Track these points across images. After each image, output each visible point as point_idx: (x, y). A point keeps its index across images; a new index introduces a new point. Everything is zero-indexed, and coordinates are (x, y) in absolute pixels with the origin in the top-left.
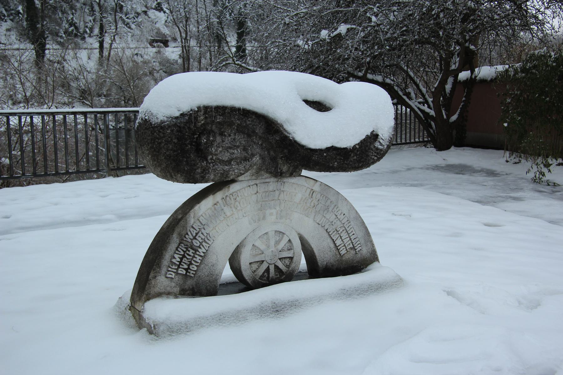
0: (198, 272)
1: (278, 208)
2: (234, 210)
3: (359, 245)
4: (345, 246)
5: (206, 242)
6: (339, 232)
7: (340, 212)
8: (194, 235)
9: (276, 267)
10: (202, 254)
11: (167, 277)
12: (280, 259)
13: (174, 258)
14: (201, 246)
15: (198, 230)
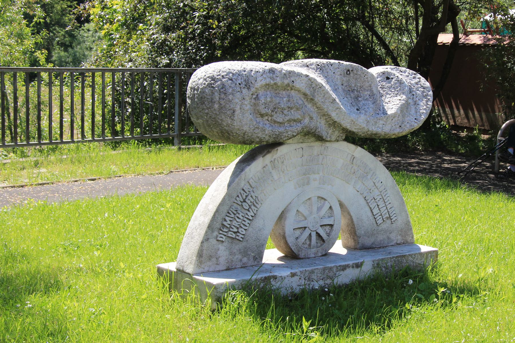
0: (246, 237)
1: (321, 174)
2: (281, 173)
3: (395, 215)
4: (381, 215)
5: (255, 206)
6: (377, 201)
7: (377, 180)
8: (244, 197)
9: (318, 235)
10: (251, 218)
11: (218, 240)
12: (321, 226)
13: (225, 220)
14: (250, 210)
15: (248, 192)
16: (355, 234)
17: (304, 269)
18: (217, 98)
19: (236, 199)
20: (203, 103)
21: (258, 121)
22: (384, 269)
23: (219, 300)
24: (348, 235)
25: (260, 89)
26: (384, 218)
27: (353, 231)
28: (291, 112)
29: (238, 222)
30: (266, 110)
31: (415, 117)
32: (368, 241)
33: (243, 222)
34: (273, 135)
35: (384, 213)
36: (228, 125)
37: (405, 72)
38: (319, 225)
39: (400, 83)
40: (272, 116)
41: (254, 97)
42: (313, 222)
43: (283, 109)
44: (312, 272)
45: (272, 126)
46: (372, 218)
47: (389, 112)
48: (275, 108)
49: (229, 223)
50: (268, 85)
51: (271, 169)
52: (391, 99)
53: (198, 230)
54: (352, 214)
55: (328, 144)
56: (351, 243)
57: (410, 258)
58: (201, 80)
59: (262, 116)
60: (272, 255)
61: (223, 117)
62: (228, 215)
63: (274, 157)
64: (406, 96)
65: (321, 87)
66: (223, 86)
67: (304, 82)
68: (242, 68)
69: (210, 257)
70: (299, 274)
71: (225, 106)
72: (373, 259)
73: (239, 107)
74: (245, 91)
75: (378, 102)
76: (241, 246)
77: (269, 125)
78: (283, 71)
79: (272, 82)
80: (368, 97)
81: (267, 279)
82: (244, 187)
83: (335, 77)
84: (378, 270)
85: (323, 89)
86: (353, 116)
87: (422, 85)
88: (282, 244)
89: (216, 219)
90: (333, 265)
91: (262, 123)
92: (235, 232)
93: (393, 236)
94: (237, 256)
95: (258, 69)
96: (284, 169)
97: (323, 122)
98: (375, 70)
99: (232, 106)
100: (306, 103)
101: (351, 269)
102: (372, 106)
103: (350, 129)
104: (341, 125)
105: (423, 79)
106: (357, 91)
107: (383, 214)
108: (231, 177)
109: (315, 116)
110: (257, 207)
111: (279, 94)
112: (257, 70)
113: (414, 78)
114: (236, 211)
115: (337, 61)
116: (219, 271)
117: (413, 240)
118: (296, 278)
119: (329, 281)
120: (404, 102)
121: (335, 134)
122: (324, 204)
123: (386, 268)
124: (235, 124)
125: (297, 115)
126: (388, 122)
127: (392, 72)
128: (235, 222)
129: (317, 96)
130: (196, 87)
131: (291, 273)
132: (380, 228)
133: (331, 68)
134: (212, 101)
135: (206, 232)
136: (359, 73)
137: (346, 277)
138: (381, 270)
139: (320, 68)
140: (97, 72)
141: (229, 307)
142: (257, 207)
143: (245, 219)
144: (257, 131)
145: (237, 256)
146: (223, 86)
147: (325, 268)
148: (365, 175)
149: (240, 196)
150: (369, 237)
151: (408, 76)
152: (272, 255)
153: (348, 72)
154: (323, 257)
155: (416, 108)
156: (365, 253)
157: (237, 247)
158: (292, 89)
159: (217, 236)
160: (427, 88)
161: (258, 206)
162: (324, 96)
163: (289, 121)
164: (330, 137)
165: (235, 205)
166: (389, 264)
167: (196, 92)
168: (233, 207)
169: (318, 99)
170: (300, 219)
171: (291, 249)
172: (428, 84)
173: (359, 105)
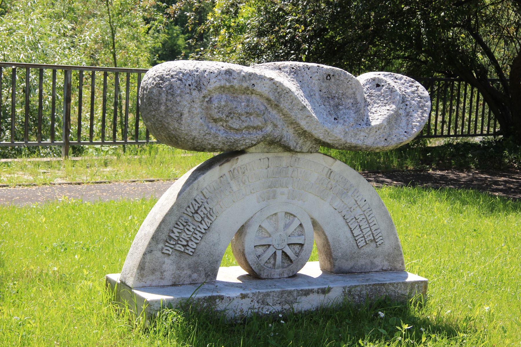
0: (197, 251)
1: (290, 187)
2: (241, 185)
3: (381, 238)
4: (364, 237)
5: (208, 218)
6: (359, 221)
7: (360, 198)
8: (196, 208)
9: (284, 254)
10: (203, 231)
11: (163, 253)
12: (289, 245)
13: (173, 232)
14: (203, 222)
15: (201, 203)
16: (331, 255)
17: (258, 291)
18: (164, 99)
19: (186, 210)
20: (150, 104)
21: (210, 126)
22: (357, 297)
23: (151, 317)
24: (324, 256)
25: (213, 91)
26: (367, 240)
27: (329, 253)
28: (250, 118)
29: (187, 234)
30: (220, 114)
31: (405, 130)
32: (347, 265)
33: (194, 235)
34: (227, 142)
35: (368, 234)
36: (175, 129)
37: (401, 79)
38: (286, 243)
39: (392, 92)
40: (227, 121)
41: (207, 100)
42: (279, 240)
43: (240, 115)
44: (268, 294)
45: (227, 133)
46: (351, 239)
47: (373, 124)
48: (230, 113)
49: (178, 235)
50: (224, 87)
51: (229, 179)
52: (378, 109)
53: (143, 240)
54: (327, 234)
55: (299, 155)
56: (328, 266)
57: (391, 287)
58: (151, 79)
59: (215, 121)
60: (230, 273)
61: (170, 120)
62: (176, 226)
63: (233, 167)
64: (397, 106)
65: (288, 92)
66: (171, 86)
67: (267, 86)
68: (195, 68)
69: (153, 271)
70: (251, 295)
71: (171, 109)
72: (343, 285)
73: (187, 110)
74: (195, 93)
75: (362, 111)
76: (191, 260)
77: (223, 132)
78: (242, 73)
79: (227, 84)
80: (350, 105)
81: (212, 299)
82: (196, 197)
83: (312, 82)
84: (349, 298)
85: (290, 94)
86: (328, 126)
87: (420, 94)
88: (243, 262)
89: (162, 229)
90: (293, 289)
91: (214, 129)
92: (183, 246)
93: (377, 261)
94: (185, 272)
95: (213, 69)
96: (245, 180)
97: (291, 131)
98: (364, 78)
99: (179, 109)
100: (270, 109)
101: (316, 295)
102: (353, 115)
103: (324, 140)
104: (312, 135)
105: (421, 88)
106: (338, 98)
107: (366, 236)
108: (183, 185)
109: (280, 124)
110: (211, 220)
111: (237, 97)
112: (211, 71)
113: (411, 86)
114: (186, 222)
115: (315, 65)
116: (163, 286)
117: (403, 267)
118: (247, 301)
119: (287, 307)
120: (392, 112)
121: (308, 145)
122: (293, 221)
123: (360, 297)
124: (183, 129)
125: (257, 122)
126: (371, 134)
127: (385, 78)
128: (184, 234)
129: (283, 102)
130: (145, 87)
131: (241, 294)
132: (362, 251)
133: (308, 72)
134: (159, 103)
135: (150, 243)
136: (342, 78)
137: (308, 303)
138: (354, 298)
139: (294, 72)
140: (59, 69)
141: (163, 325)
142: (211, 220)
143: (197, 232)
144: (207, 137)
145: (185, 272)
146: (171, 86)
147: (283, 291)
148: (345, 191)
149: (191, 206)
150: (347, 260)
151: (403, 84)
152: (230, 273)
153: (328, 76)
154: (290, 279)
155: (408, 120)
156: (340, 278)
157: (186, 262)
158: (252, 93)
159: (163, 248)
160: (425, 97)
161: (213, 219)
162: (292, 103)
163: (248, 128)
164: (301, 148)
165: (185, 216)
166: (364, 292)
167: (145, 92)
168: (183, 219)
169: (284, 105)
170: (263, 236)
171: (251, 268)
172: (426, 93)
173: (339, 114)
